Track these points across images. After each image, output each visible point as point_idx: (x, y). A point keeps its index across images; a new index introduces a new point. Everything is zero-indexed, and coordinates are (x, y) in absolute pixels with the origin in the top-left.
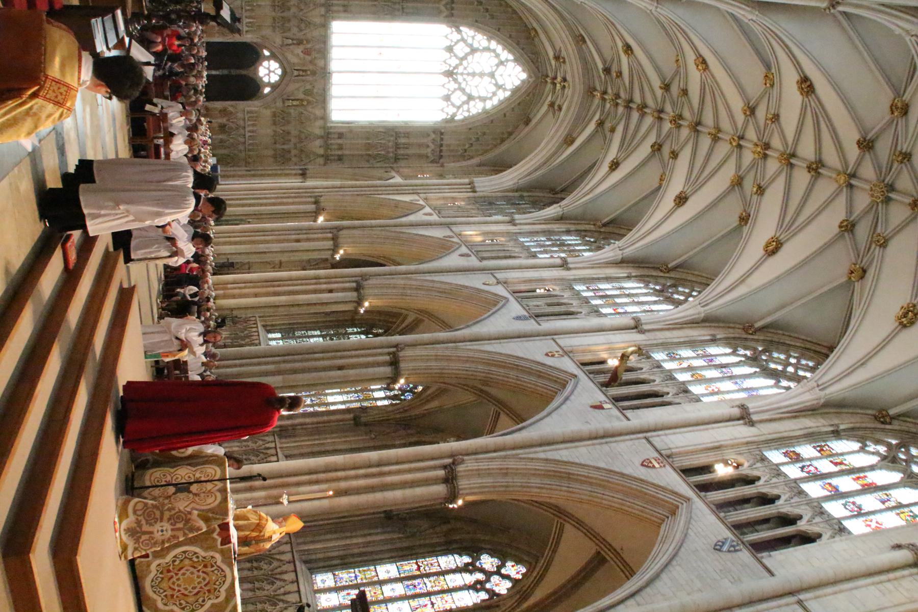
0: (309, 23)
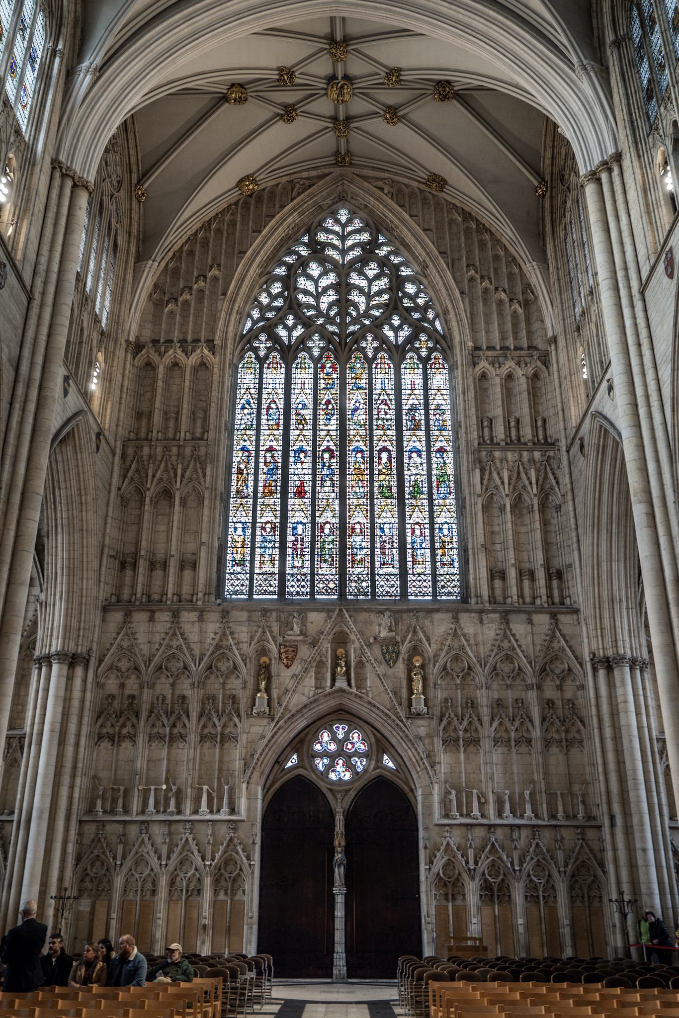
0: (218, 647)
